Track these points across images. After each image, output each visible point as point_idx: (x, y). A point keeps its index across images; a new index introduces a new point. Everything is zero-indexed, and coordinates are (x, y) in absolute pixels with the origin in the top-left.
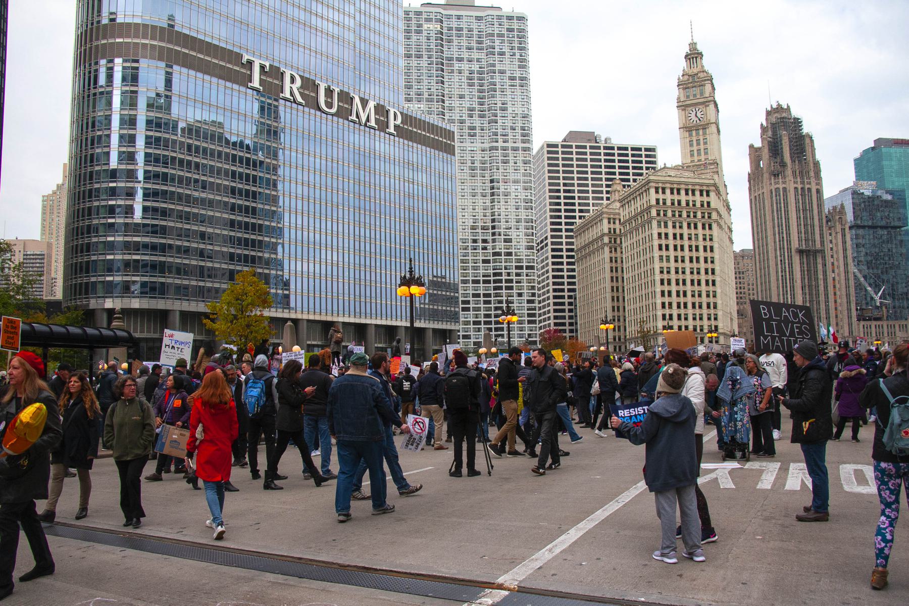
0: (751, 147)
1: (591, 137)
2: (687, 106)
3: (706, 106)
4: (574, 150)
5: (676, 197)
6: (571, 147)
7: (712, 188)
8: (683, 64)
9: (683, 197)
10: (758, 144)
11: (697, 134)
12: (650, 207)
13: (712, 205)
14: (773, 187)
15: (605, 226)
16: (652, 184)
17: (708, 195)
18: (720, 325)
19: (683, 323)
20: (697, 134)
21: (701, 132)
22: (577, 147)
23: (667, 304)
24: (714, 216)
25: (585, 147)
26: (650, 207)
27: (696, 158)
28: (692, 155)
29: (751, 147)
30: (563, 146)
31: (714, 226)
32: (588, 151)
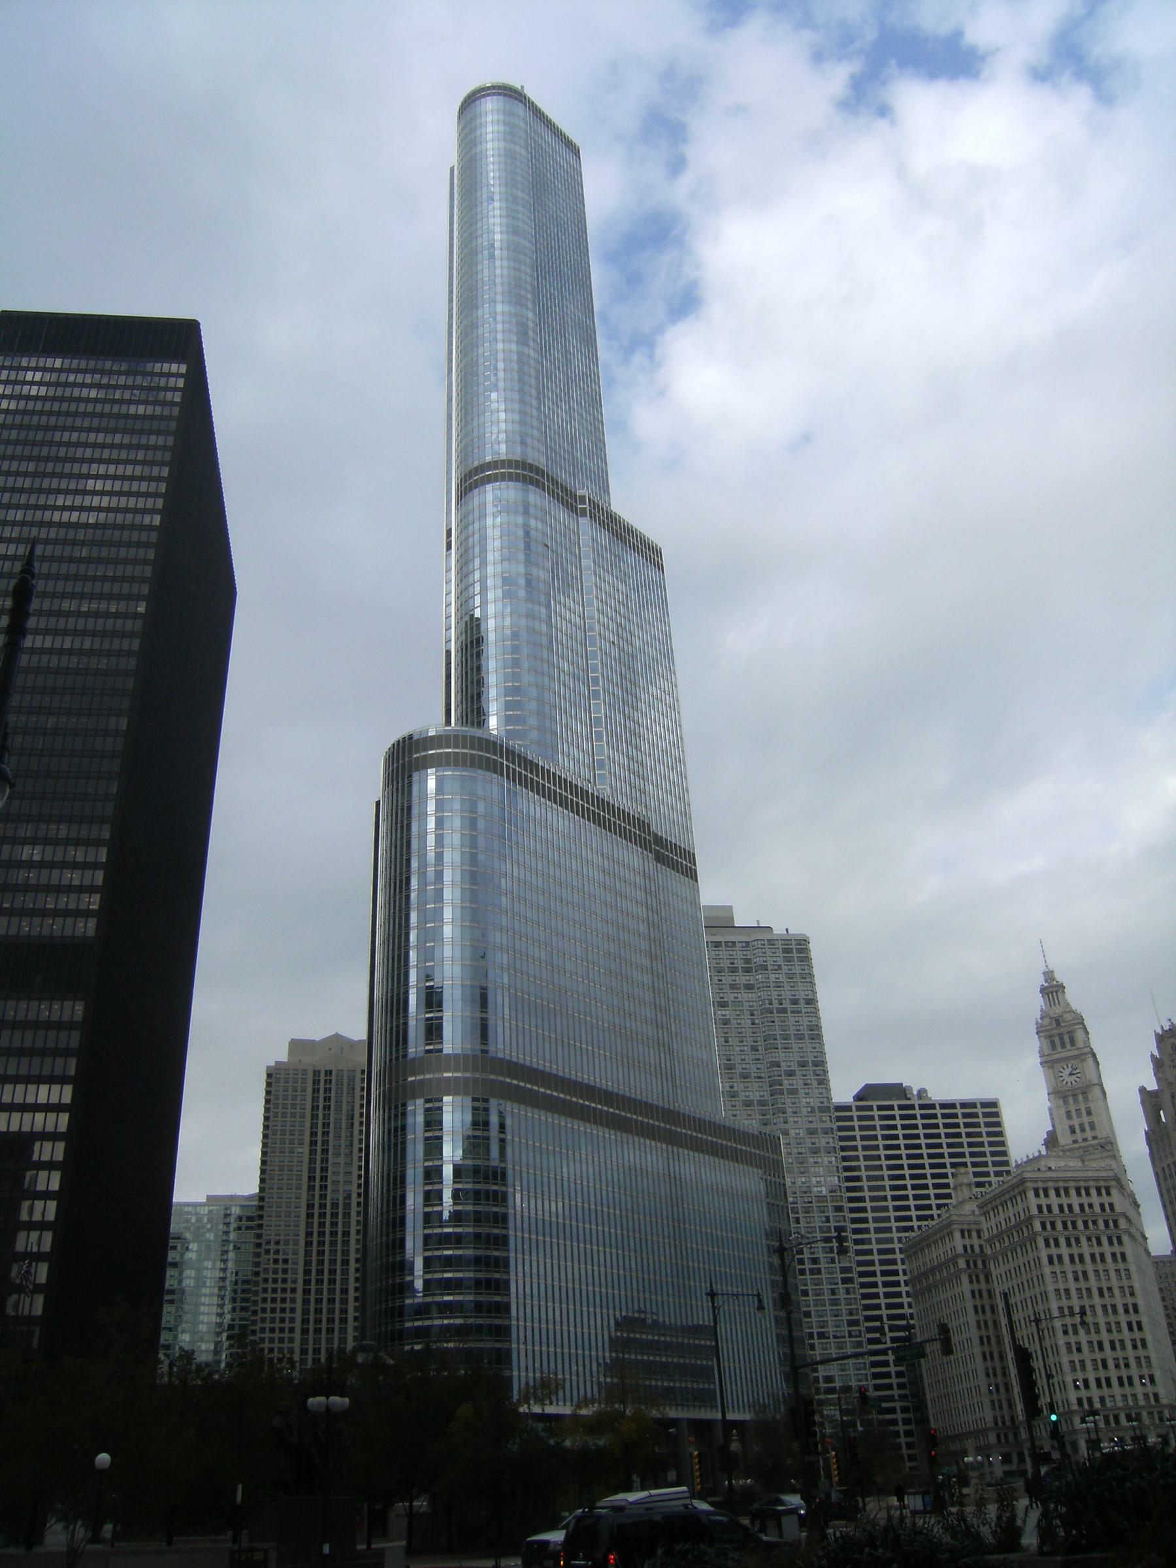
0: (1142, 1090)
1: (898, 1091)
3: (1082, 1061)
4: (876, 1113)
6: (870, 1108)
7: (1113, 1183)
8: (1039, 1001)
9: (1075, 1200)
10: (1152, 1085)
11: (1076, 1101)
12: (1031, 1218)
13: (1118, 1208)
15: (958, 1242)
17: (1108, 1194)
18: (1162, 1392)
20: (1076, 1101)
21: (1080, 1097)
22: (880, 1108)
23: (1077, 1363)
24: (1122, 1224)
25: (891, 1108)
26: (1031, 1218)
27: (1079, 1136)
28: (1073, 1131)
29: (1142, 1090)
30: (859, 1108)
31: (1125, 1238)
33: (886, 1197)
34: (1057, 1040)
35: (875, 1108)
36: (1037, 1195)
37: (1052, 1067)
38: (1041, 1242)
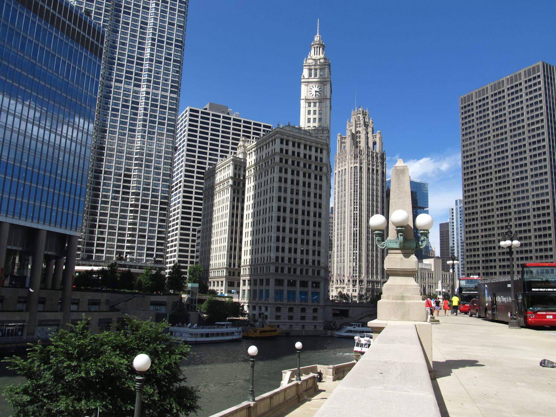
2: (309, 82)
3: (325, 85)
4: (211, 117)
5: (296, 150)
6: (209, 114)
7: (325, 147)
9: (302, 151)
13: (324, 160)
14: (352, 165)
16: (277, 135)
17: (321, 152)
19: (293, 255)
22: (213, 115)
25: (219, 116)
26: (275, 154)
32: (221, 119)
33: (206, 158)
34: (313, 72)
35: (211, 115)
36: (282, 142)
37: (307, 85)
38: (277, 169)
